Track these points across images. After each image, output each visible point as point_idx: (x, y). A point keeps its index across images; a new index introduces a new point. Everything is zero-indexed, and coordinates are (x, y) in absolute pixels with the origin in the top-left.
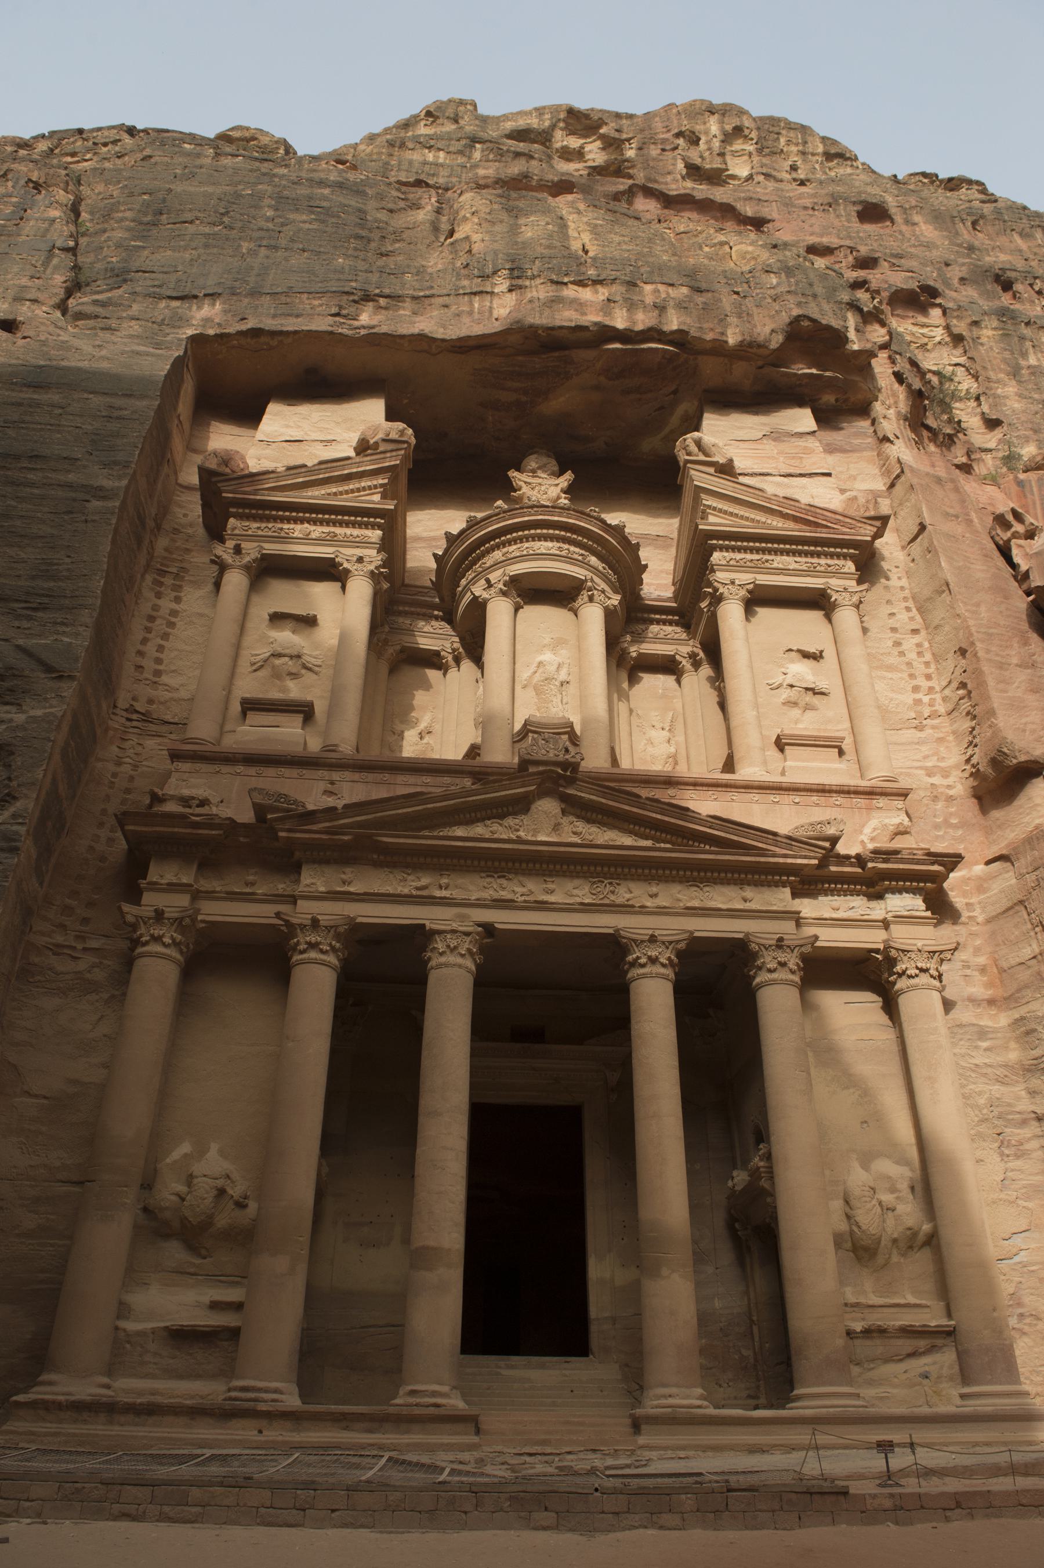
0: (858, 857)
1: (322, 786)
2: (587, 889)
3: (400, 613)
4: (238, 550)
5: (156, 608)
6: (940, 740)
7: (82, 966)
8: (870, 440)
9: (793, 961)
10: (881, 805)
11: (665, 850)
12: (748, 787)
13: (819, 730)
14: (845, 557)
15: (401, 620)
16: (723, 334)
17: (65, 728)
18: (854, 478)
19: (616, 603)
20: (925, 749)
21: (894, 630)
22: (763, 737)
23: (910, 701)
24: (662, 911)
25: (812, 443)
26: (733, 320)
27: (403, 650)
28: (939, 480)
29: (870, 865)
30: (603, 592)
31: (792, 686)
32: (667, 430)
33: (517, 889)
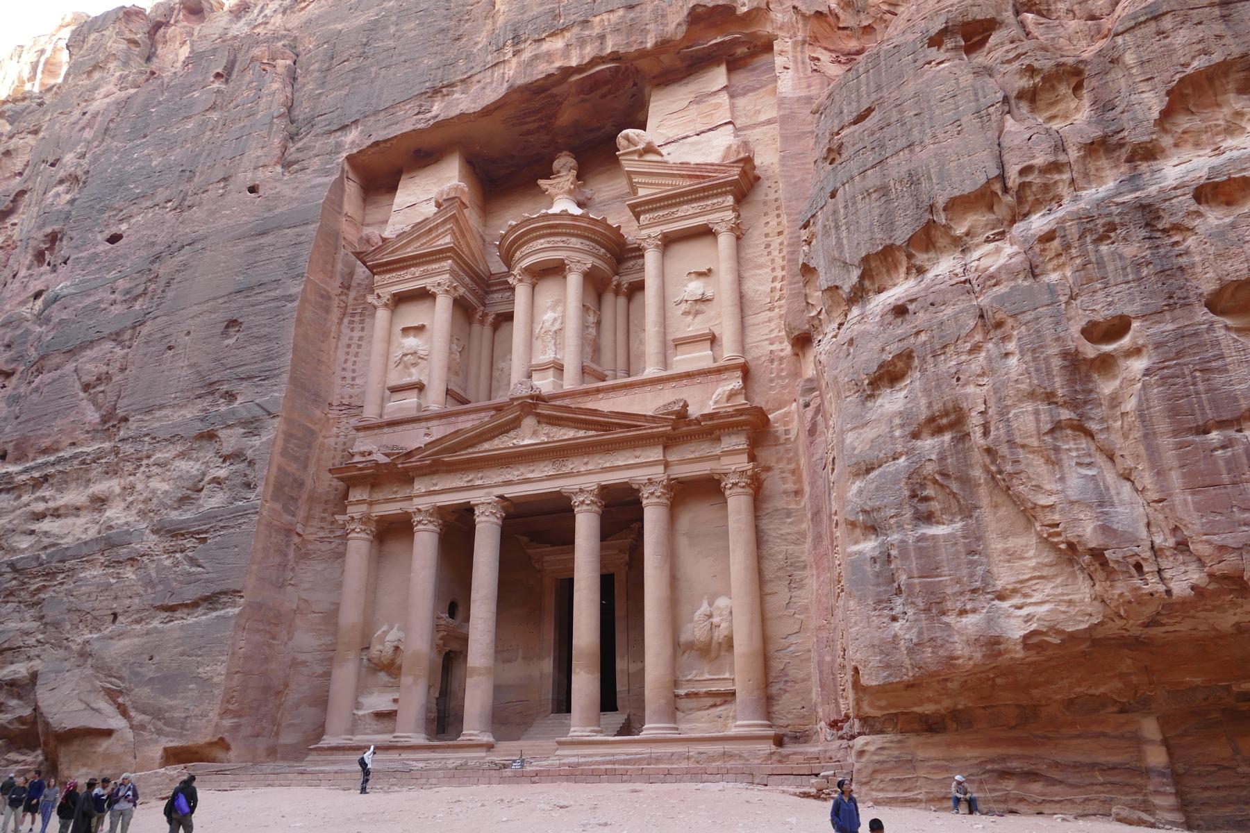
1: (424, 431)
3: (496, 291)
4: (379, 297)
5: (351, 339)
6: (781, 317)
7: (334, 545)
12: (644, 383)
14: (725, 193)
15: (495, 296)
17: (280, 443)
18: (758, 112)
20: (772, 325)
21: (767, 235)
25: (724, 98)
26: (652, 26)
27: (498, 315)
33: (514, 474)
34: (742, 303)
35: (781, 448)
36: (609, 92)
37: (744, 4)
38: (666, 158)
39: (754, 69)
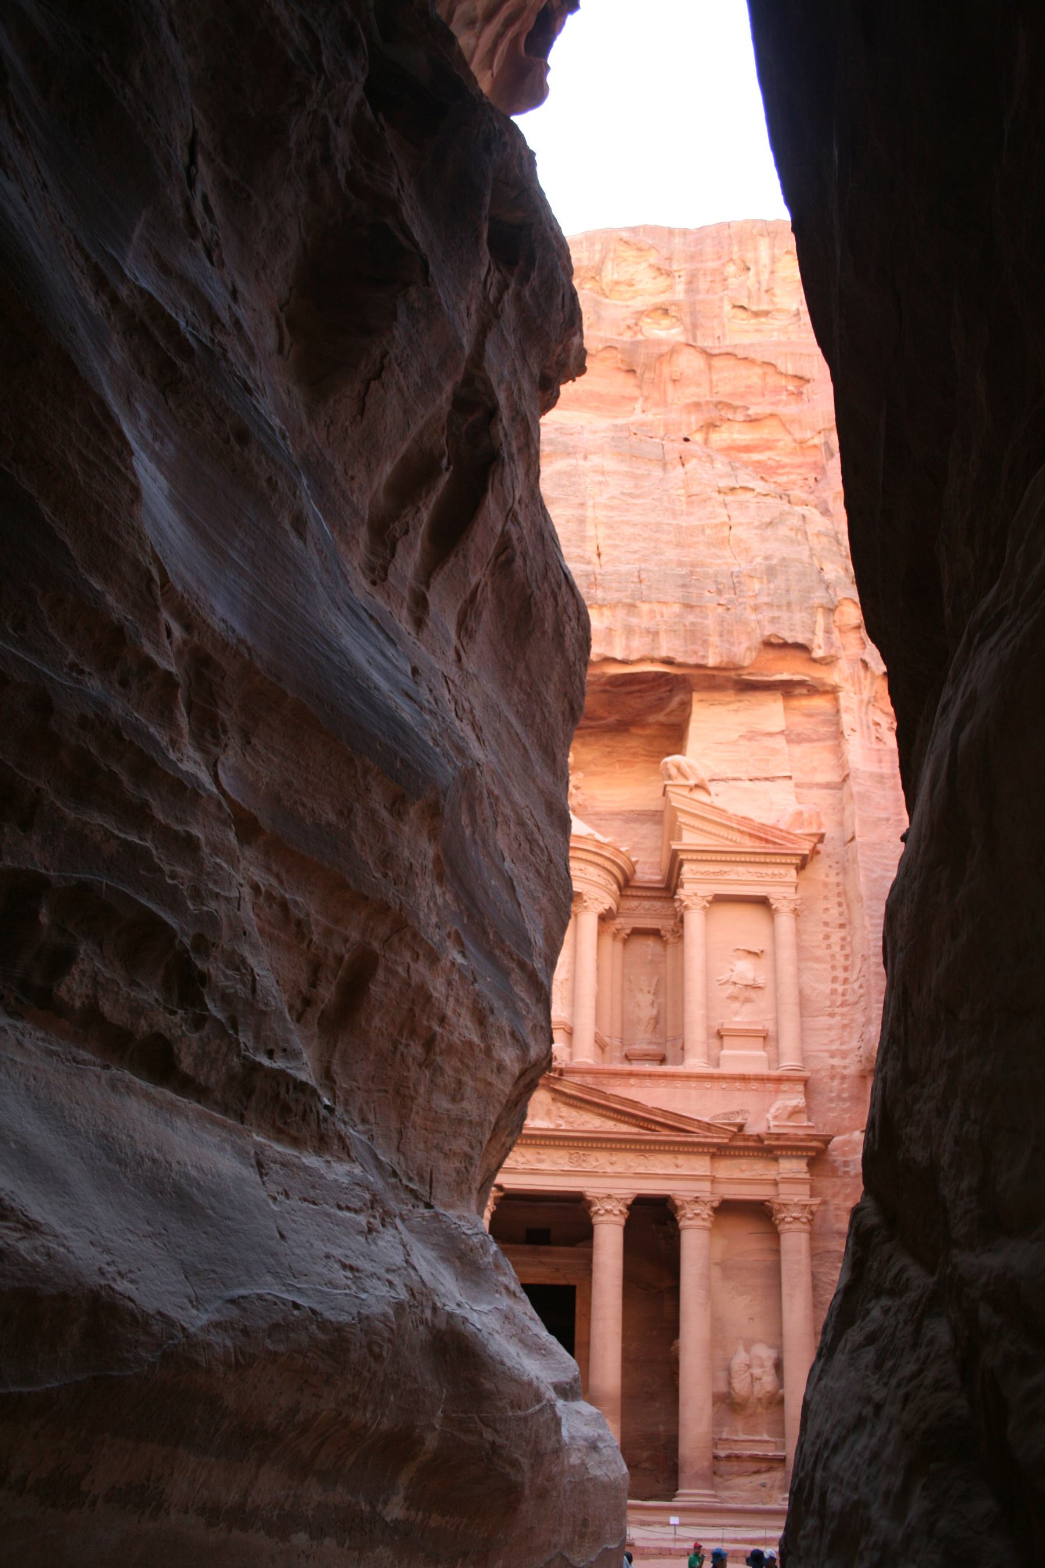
0: (758, 1136)
2: (567, 1157)
6: (844, 1026)
8: (833, 729)
9: (706, 1212)
10: (786, 1089)
11: (624, 1129)
12: (689, 1077)
13: (749, 1023)
16: (704, 657)
18: (815, 769)
19: (607, 907)
20: (833, 1034)
21: (826, 924)
22: (708, 1028)
23: (828, 991)
24: (618, 1176)
25: (780, 743)
26: (714, 639)
28: (880, 779)
29: (766, 1142)
30: (596, 899)
31: (735, 983)
32: (668, 710)
34: (803, 1002)
35: (839, 1182)
36: (640, 691)
37: (820, 647)
38: (718, 802)
39: (811, 716)
